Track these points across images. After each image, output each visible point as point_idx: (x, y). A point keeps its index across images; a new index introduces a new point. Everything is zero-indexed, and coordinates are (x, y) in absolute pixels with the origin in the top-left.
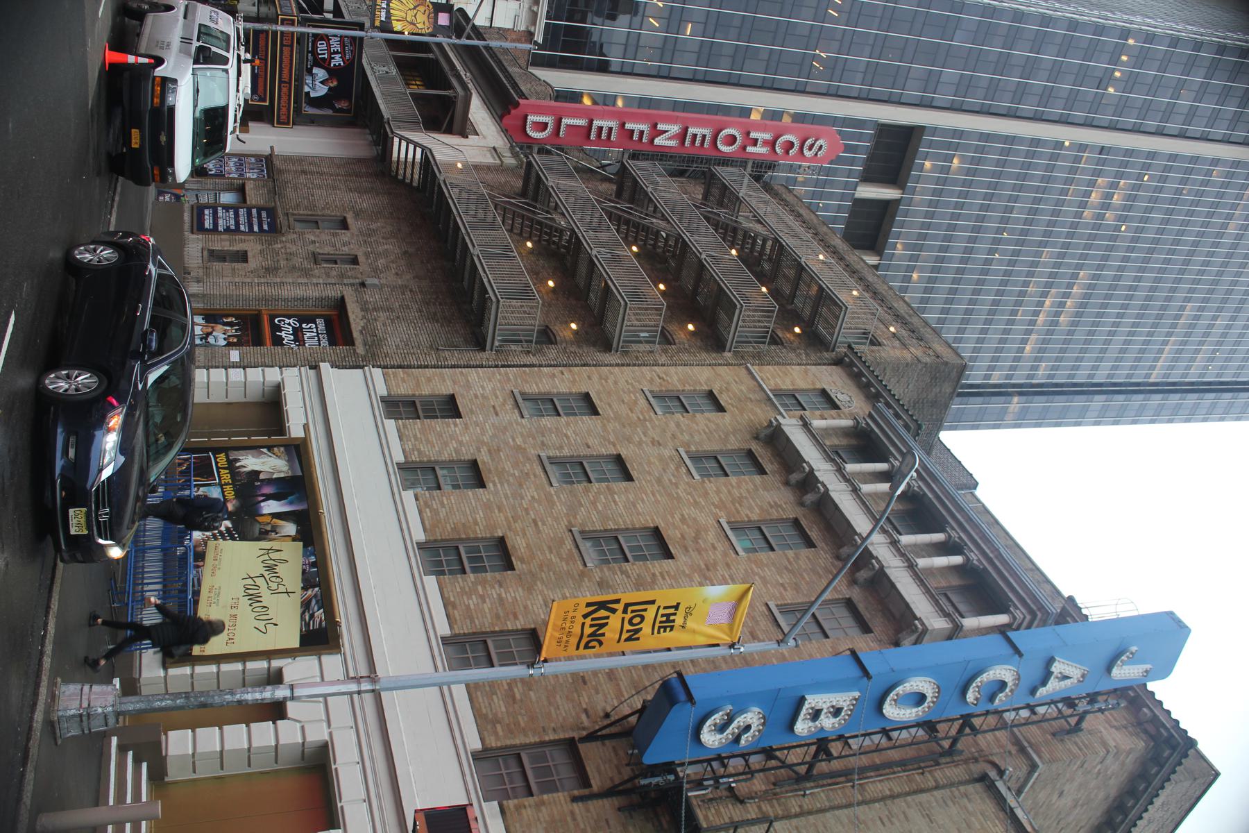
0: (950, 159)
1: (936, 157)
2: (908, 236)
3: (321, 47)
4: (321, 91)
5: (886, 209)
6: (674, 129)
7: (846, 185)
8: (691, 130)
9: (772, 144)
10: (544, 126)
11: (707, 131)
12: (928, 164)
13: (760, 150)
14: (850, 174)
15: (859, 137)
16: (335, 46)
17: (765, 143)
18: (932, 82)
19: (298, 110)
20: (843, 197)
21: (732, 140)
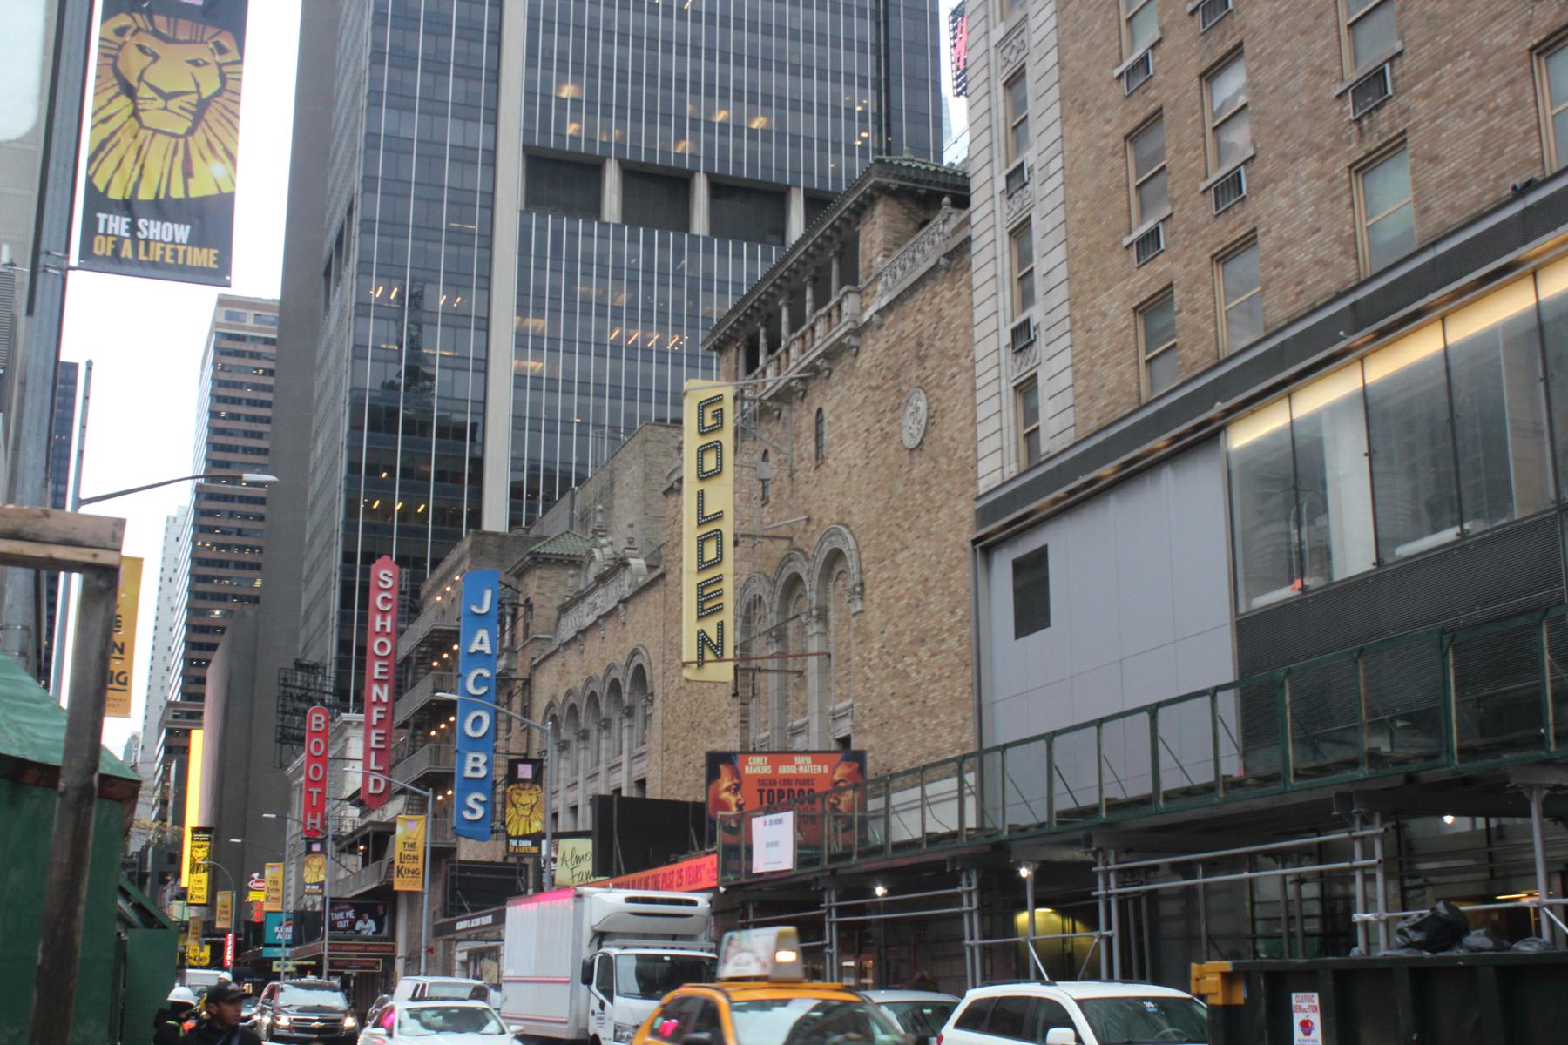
0: (561, 102)
1: (561, 124)
2: (665, 140)
3: (341, 925)
4: (371, 924)
5: (633, 174)
6: (376, 689)
7: (603, 237)
8: (376, 676)
9: (384, 613)
10: (377, 782)
11: (377, 663)
12: (571, 129)
13: (388, 623)
14: (588, 235)
15: (542, 229)
16: (340, 915)
17: (383, 619)
18: (464, 157)
19: (386, 939)
20: (619, 238)
21: (382, 645)
